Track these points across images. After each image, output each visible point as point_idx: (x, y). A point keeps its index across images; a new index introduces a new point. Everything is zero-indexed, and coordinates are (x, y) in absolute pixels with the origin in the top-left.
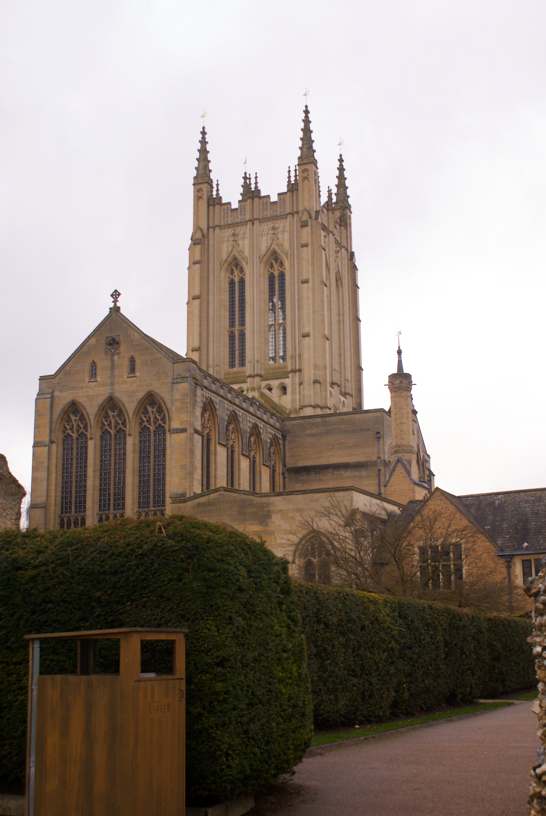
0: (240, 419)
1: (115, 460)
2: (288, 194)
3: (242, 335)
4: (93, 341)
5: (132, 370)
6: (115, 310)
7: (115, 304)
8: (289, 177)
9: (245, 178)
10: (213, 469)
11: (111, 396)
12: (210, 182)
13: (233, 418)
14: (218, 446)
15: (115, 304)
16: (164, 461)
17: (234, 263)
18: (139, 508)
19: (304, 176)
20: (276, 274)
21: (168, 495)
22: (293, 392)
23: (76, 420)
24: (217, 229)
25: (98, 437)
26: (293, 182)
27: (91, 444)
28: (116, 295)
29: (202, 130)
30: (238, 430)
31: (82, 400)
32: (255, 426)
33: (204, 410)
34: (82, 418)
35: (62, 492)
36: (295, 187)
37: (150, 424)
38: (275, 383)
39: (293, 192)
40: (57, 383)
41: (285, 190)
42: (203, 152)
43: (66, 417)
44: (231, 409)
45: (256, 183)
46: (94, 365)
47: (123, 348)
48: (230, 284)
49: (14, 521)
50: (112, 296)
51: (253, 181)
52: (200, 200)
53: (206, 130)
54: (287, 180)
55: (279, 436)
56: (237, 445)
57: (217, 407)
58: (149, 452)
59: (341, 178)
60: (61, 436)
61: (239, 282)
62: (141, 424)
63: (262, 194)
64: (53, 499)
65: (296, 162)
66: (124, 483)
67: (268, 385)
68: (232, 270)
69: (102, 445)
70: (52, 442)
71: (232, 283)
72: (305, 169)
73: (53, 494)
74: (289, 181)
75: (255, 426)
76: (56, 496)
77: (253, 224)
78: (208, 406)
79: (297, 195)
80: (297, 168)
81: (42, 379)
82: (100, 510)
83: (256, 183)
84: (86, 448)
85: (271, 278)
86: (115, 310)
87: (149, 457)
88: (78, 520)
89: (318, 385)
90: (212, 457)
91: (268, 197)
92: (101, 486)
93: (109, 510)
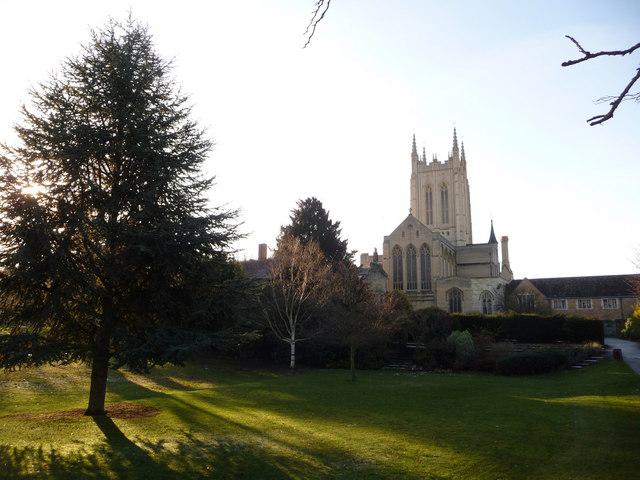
3: (431, 212)
5: (418, 235)
38: (445, 231)
41: (447, 159)
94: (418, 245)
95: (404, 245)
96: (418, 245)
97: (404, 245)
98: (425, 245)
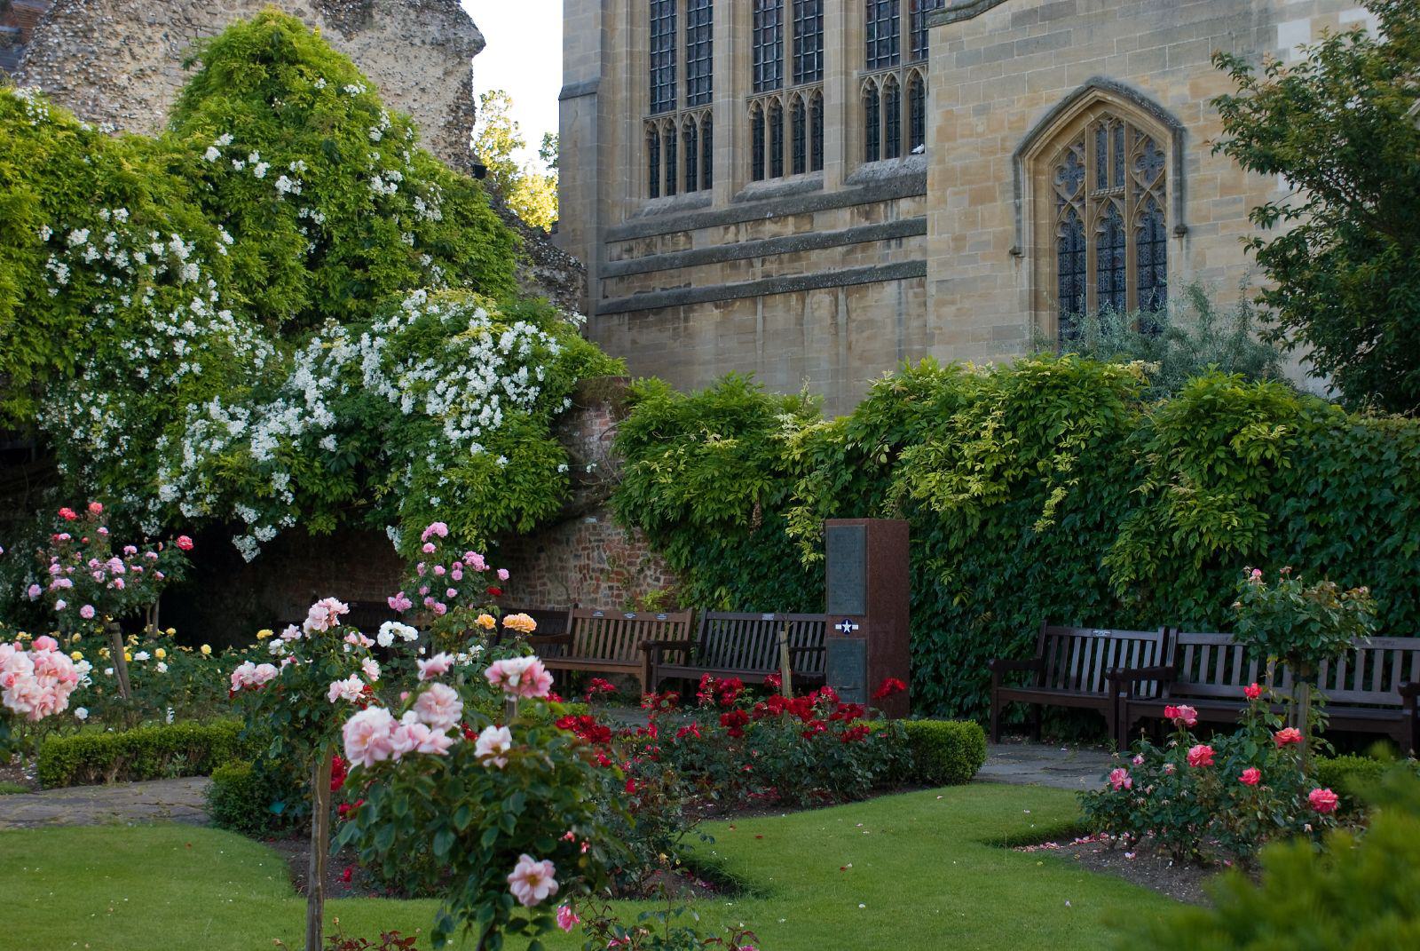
18: (869, 65)
35: (653, 40)
49: (444, 134)
64: (622, 64)
73: (621, 48)
76: (631, 55)
82: (756, 88)
88: (695, 126)
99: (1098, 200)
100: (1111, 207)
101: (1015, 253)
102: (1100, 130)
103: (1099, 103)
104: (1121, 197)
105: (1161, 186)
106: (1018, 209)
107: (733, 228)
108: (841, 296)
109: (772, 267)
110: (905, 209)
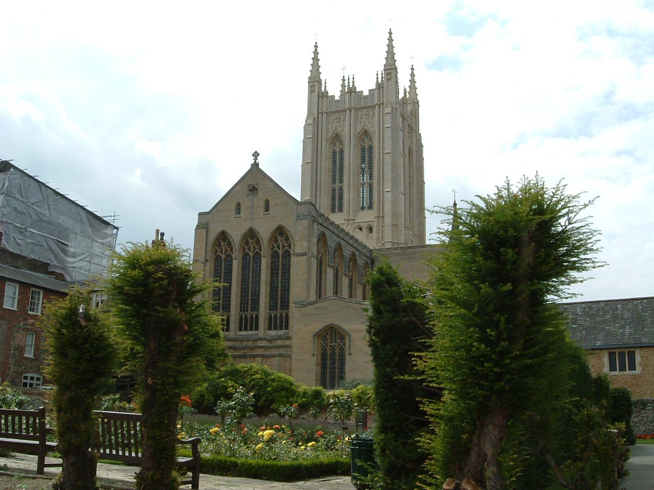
0: (343, 249)
1: (253, 274)
2: (376, 90)
4: (238, 187)
5: (267, 209)
6: (255, 165)
7: (255, 161)
8: (377, 78)
9: (344, 80)
10: (324, 284)
11: (251, 228)
12: (320, 81)
13: (339, 247)
14: (327, 267)
15: (255, 161)
16: (289, 276)
17: (336, 138)
18: (270, 310)
19: (388, 78)
20: (366, 146)
21: (291, 301)
22: (378, 232)
23: (224, 245)
24: (324, 115)
25: (241, 258)
26: (380, 82)
27: (235, 263)
28: (256, 155)
29: (315, 44)
30: (342, 256)
31: (228, 230)
32: (354, 254)
33: (319, 241)
34: (229, 244)
36: (381, 86)
37: (279, 249)
39: (380, 89)
40: (212, 218)
41: (374, 87)
42: (316, 59)
43: (217, 242)
44: (337, 240)
45: (353, 82)
46: (239, 205)
47: (261, 193)
48: (333, 153)
50: (253, 155)
51: (351, 81)
52: (313, 93)
53: (318, 45)
54: (376, 80)
55: (369, 262)
56: (340, 267)
57: (328, 238)
58: (278, 269)
59: (413, 81)
60: (214, 257)
61: (339, 152)
62: (272, 249)
63: (357, 91)
65: (383, 68)
66: (259, 291)
67: (360, 225)
68: (335, 143)
69: (243, 263)
70: (206, 261)
71: (334, 152)
72: (389, 73)
74: (377, 81)
75: (354, 254)
77: (351, 111)
78: (322, 238)
79: (383, 91)
80: (383, 72)
81: (200, 214)
82: (241, 311)
83: (353, 82)
84: (231, 265)
85: (363, 150)
86: (255, 165)
87: (278, 273)
89: (395, 227)
90: (323, 275)
91: (362, 92)
92: (241, 293)
93: (247, 311)
94: (265, 231)
95: (236, 237)
96: (265, 231)
97: (236, 237)
98: (280, 231)
99: (331, 346)
100: (333, 347)
101: (313, 355)
102: (331, 332)
103: (332, 327)
104: (336, 346)
105: (344, 344)
106: (314, 346)
107: (235, 342)
108: (264, 359)
109: (246, 351)
110: (287, 342)
